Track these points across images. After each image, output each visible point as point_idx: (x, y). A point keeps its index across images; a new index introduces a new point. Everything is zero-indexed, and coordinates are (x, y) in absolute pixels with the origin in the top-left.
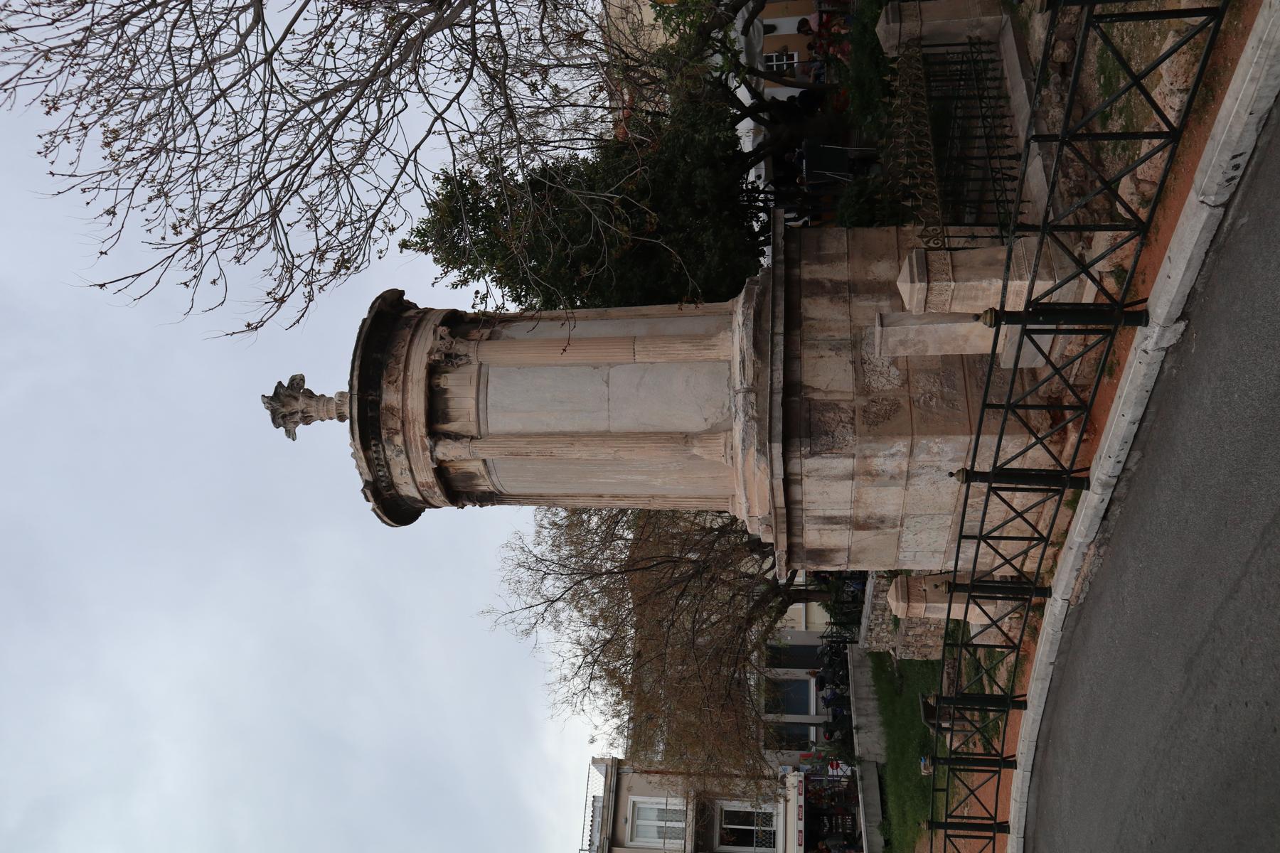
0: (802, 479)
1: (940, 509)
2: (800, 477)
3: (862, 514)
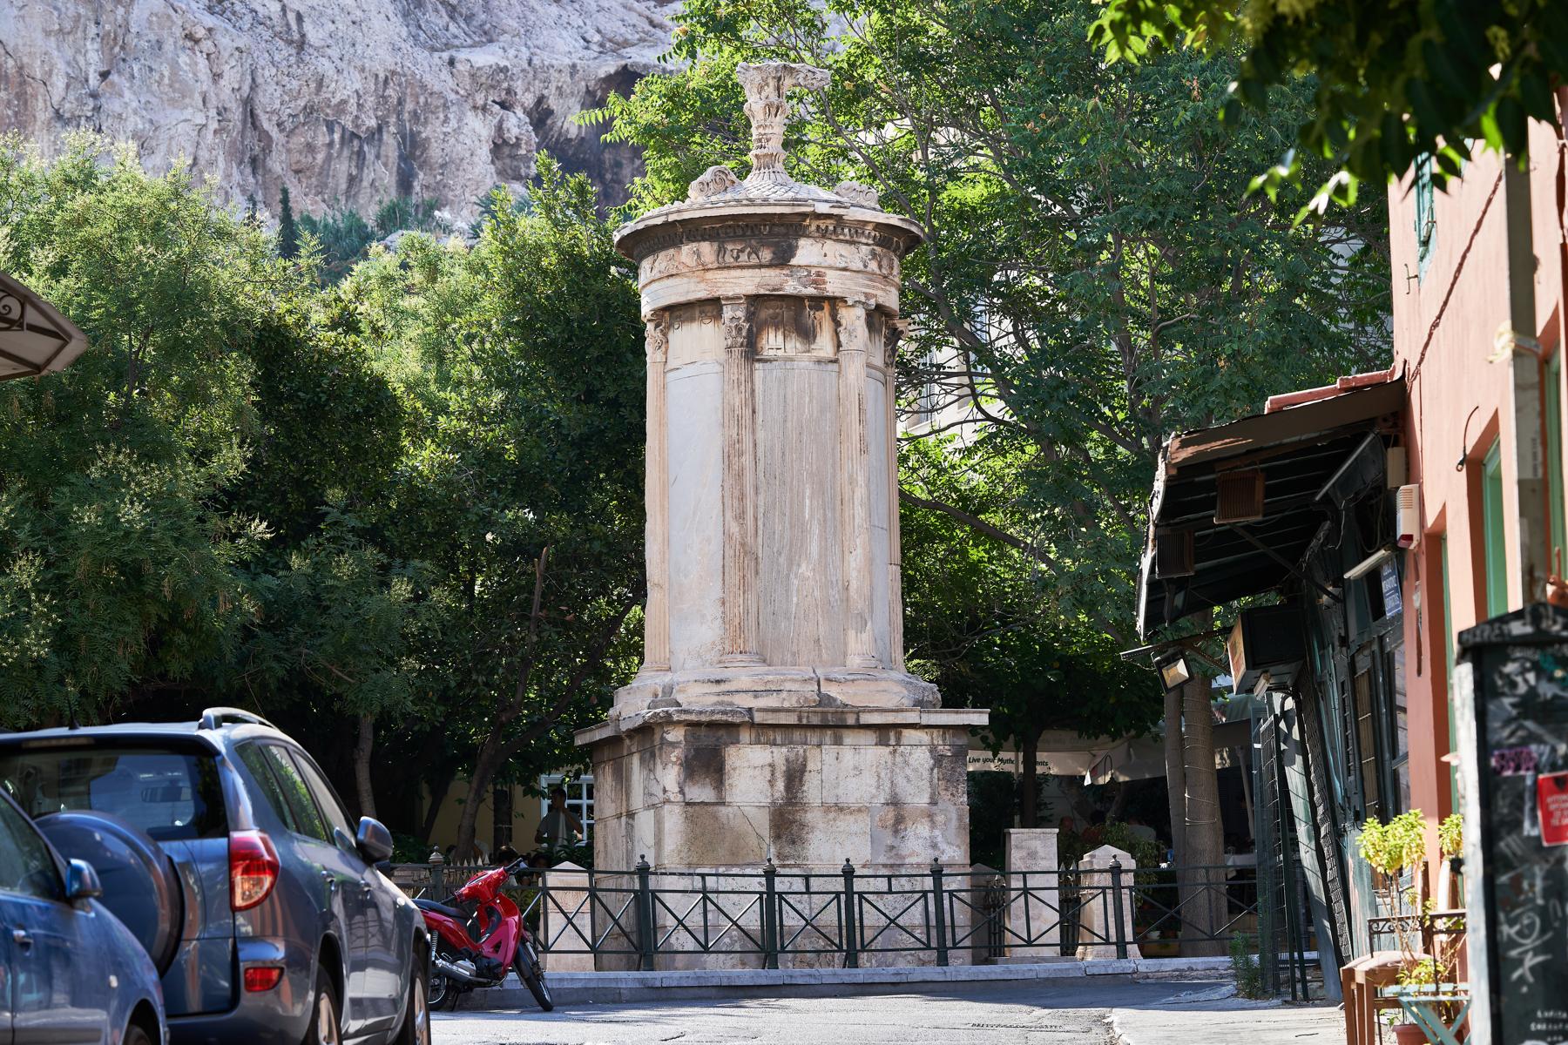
0: (888, 745)
2: (892, 742)
3: (813, 817)
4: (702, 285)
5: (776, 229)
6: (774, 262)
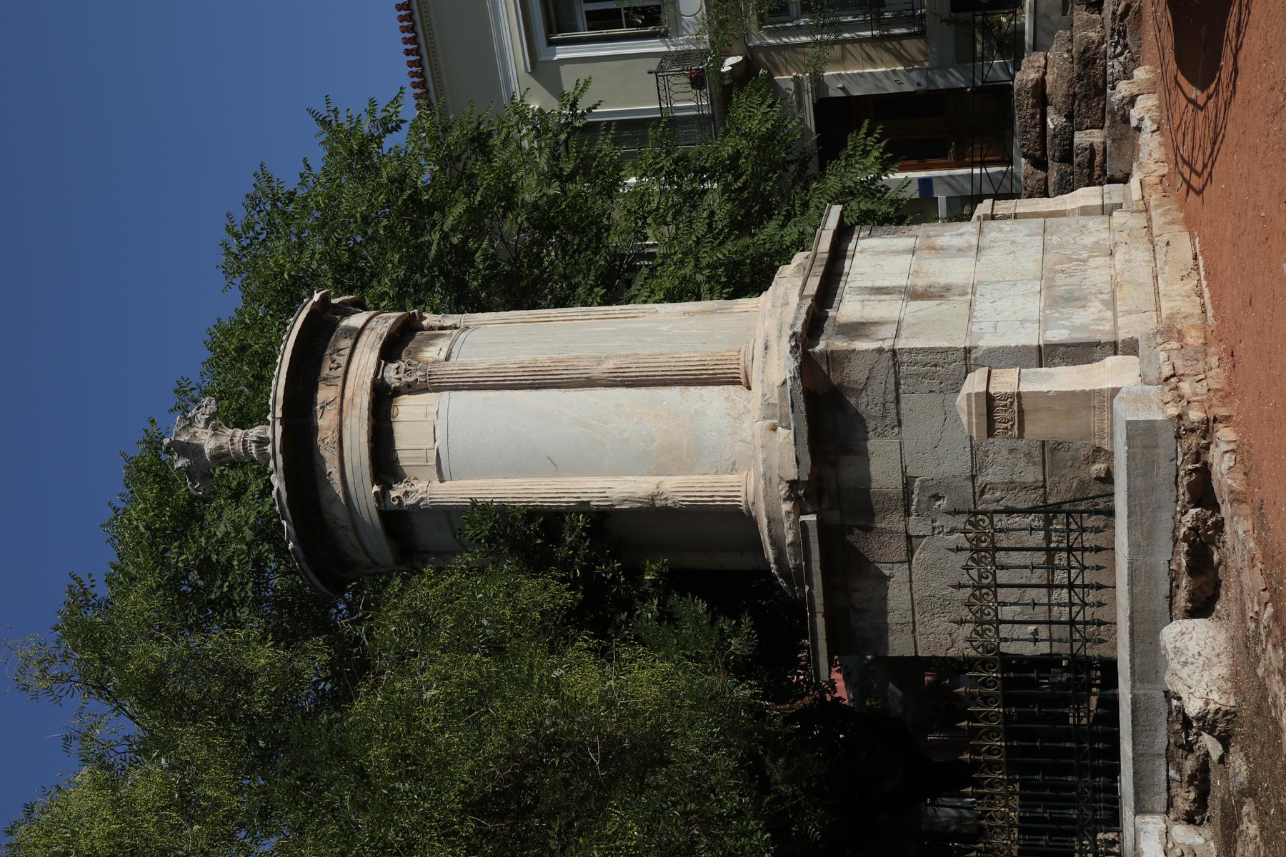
1: (1022, 275)
3: (921, 283)
4: (357, 400)
6: (354, 336)
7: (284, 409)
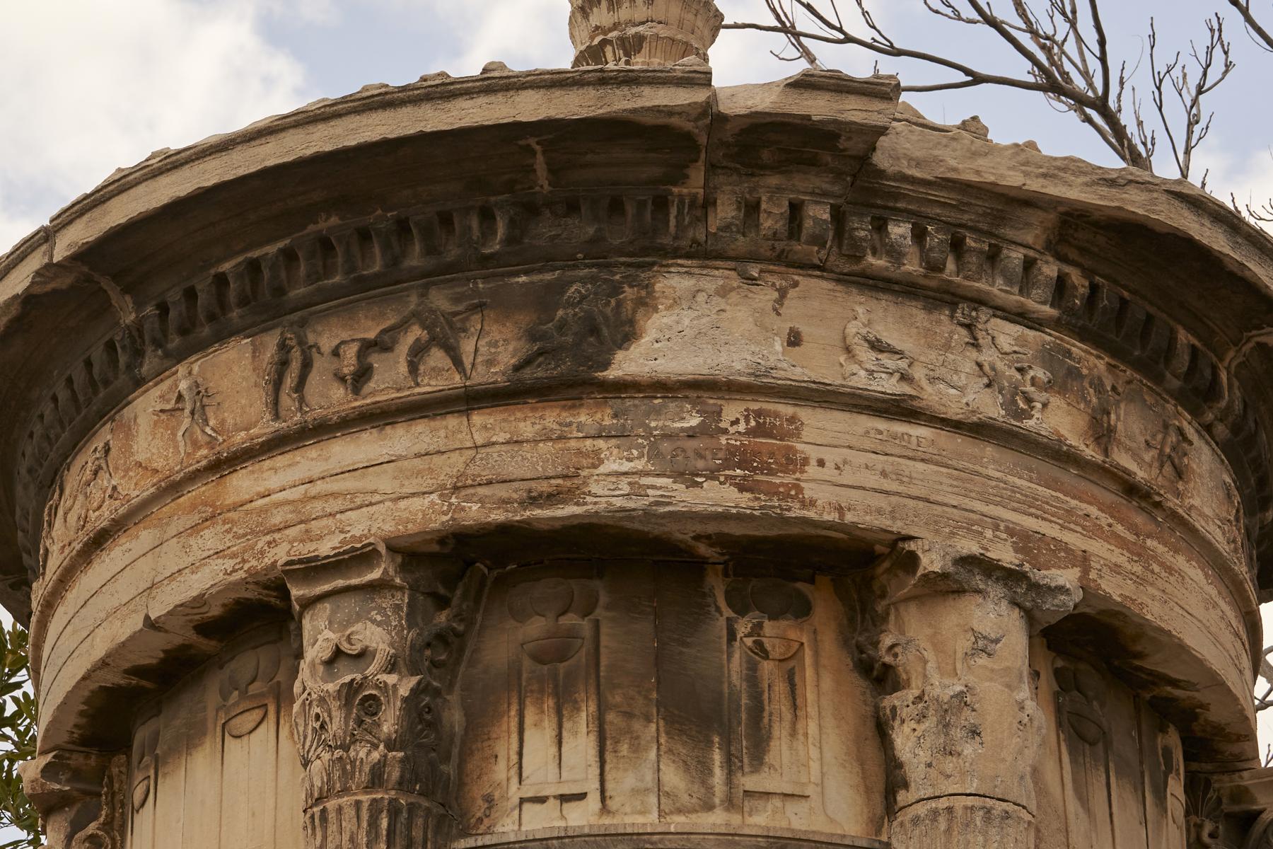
4: (210, 539)
5: (544, 231)
7: (87, 255)
